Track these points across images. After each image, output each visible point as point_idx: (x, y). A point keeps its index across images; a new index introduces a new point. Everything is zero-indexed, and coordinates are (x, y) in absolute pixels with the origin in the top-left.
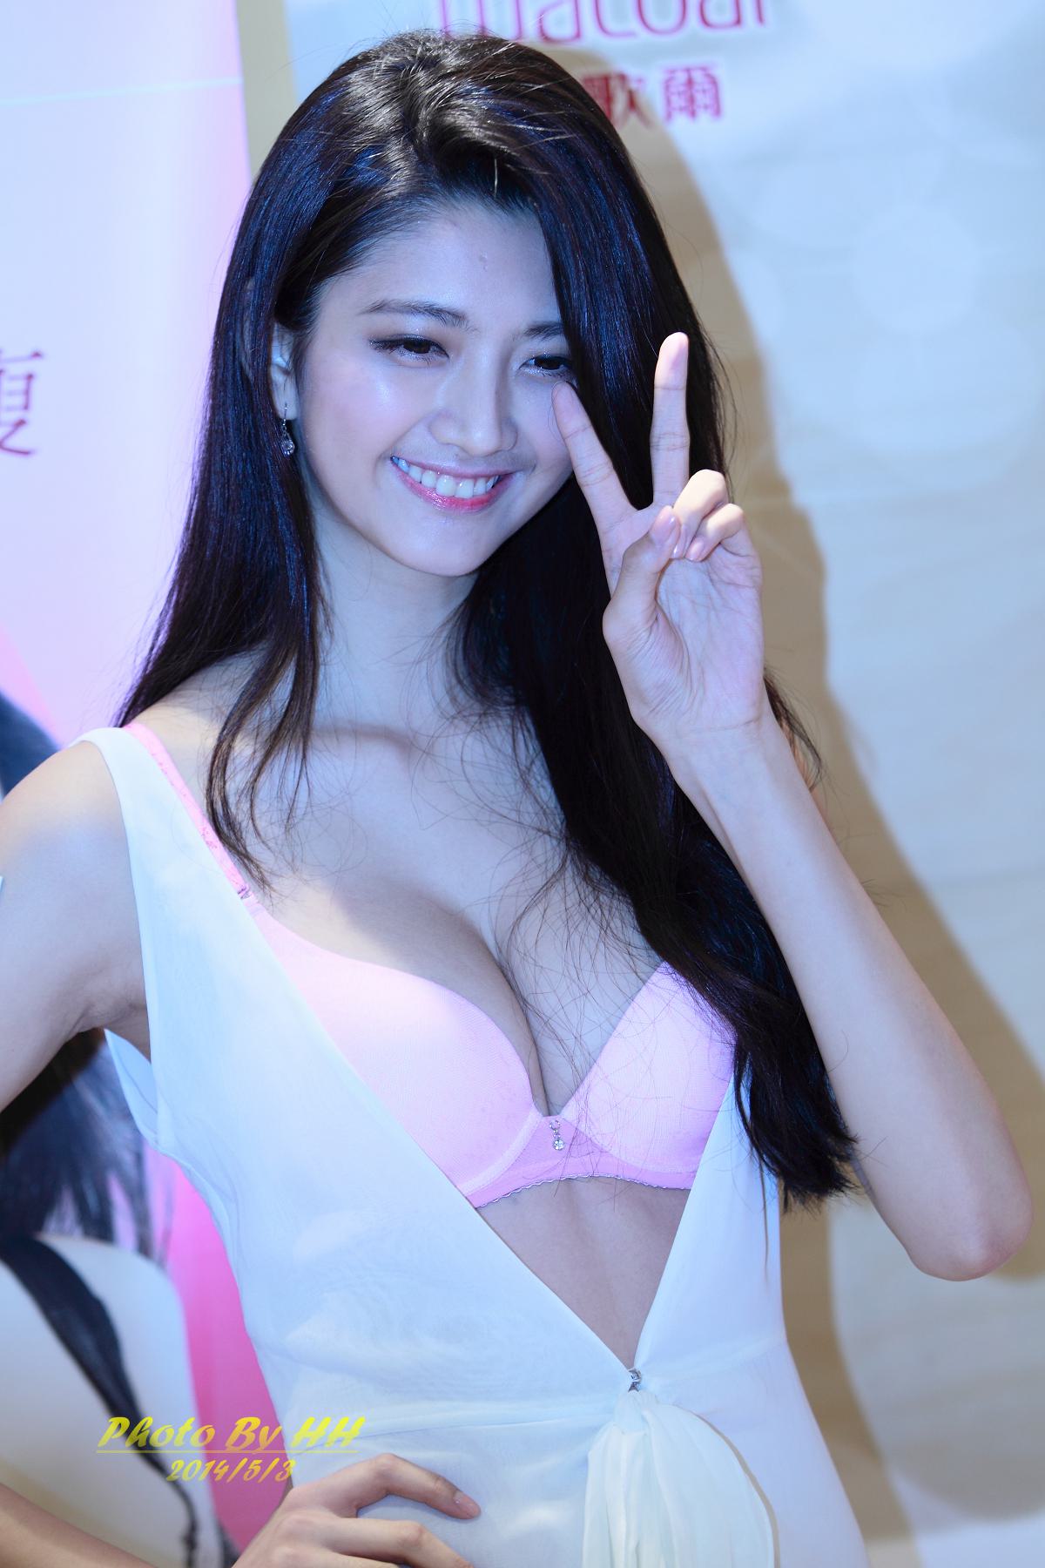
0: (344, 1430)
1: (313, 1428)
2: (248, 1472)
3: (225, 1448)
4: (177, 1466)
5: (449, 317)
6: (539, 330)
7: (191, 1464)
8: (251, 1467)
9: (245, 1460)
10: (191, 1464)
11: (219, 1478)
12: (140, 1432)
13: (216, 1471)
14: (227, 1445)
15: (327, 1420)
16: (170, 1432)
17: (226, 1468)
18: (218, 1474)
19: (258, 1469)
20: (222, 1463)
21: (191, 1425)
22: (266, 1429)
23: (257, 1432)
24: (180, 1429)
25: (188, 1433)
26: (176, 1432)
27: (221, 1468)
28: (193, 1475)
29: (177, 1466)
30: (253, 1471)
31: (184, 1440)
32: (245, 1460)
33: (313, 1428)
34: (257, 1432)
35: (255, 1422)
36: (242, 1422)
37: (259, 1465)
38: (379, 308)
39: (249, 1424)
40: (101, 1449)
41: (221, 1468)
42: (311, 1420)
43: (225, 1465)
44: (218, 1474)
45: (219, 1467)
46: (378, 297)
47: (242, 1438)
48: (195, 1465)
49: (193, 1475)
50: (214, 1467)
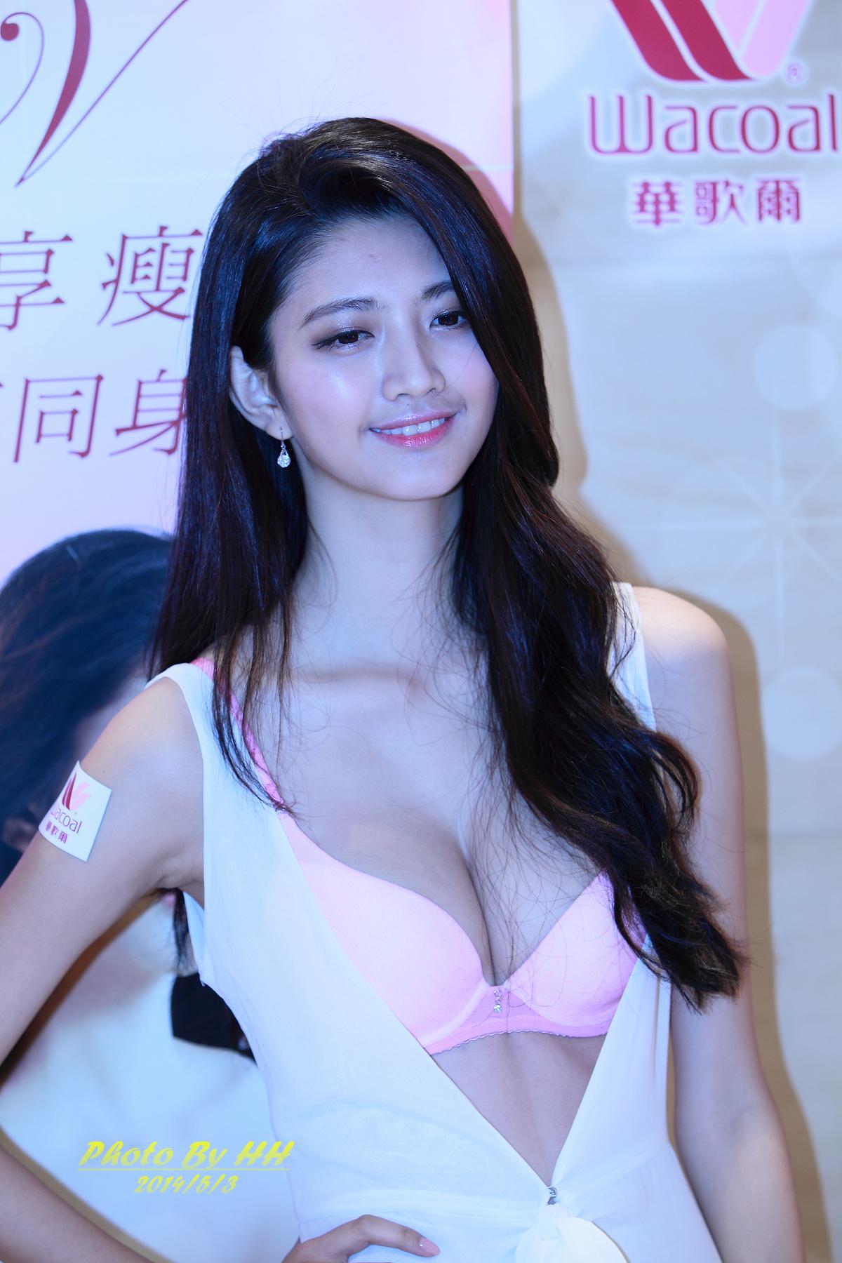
1: (253, 1150)
2: (199, 1187)
8: (203, 1181)
9: (197, 1176)
10: (154, 1179)
11: (176, 1191)
12: (113, 1153)
13: (174, 1185)
15: (263, 1144)
16: (137, 1153)
19: (208, 1184)
22: (214, 1151)
23: (207, 1153)
24: (145, 1151)
27: (178, 1182)
30: (204, 1184)
32: (197, 1176)
33: (253, 1150)
35: (206, 1145)
36: (195, 1146)
37: (210, 1180)
39: (200, 1148)
41: (178, 1182)
42: (250, 1144)
47: (195, 1159)
48: (157, 1180)
50: (173, 1181)
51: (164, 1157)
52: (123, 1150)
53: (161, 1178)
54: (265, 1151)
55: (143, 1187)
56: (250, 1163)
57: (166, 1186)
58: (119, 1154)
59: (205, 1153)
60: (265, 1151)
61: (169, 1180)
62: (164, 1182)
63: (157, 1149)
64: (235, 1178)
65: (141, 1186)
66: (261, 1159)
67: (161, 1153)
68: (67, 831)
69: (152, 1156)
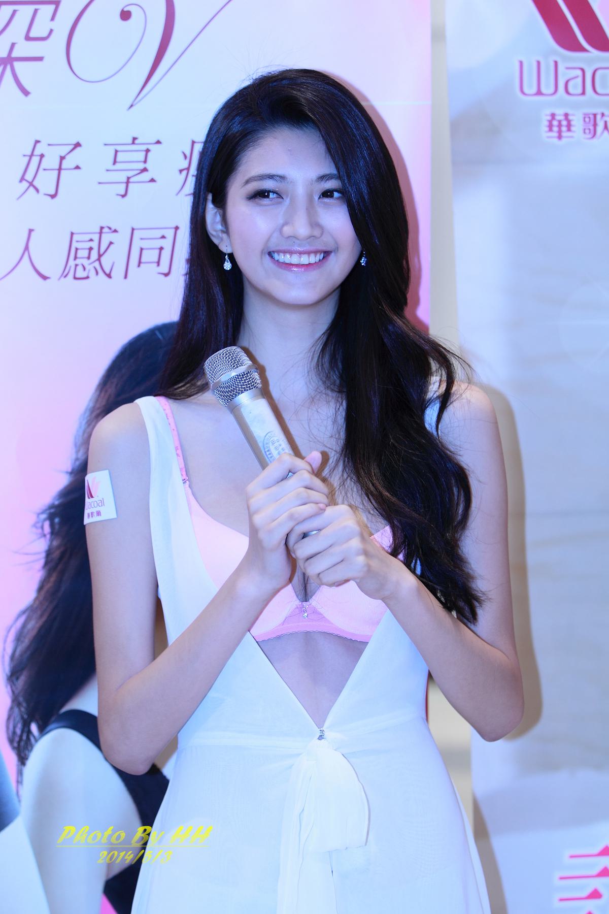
3: (131, 844)
4: (103, 854)
5: (278, 178)
6: (322, 178)
7: (111, 853)
10: (111, 853)
12: (82, 835)
13: (126, 858)
14: (132, 842)
17: (132, 855)
18: (127, 859)
21: (112, 831)
25: (109, 835)
26: (103, 835)
27: (129, 856)
29: (103, 854)
31: (107, 839)
38: (247, 182)
43: (131, 854)
45: (128, 855)
46: (246, 178)
48: (114, 854)
51: (119, 837)
52: (89, 833)
53: (116, 853)
55: (103, 859)
57: (120, 858)
58: (86, 835)
61: (122, 854)
62: (118, 855)
63: (114, 831)
64: (170, 853)
67: (117, 834)
68: (98, 509)
69: (110, 836)
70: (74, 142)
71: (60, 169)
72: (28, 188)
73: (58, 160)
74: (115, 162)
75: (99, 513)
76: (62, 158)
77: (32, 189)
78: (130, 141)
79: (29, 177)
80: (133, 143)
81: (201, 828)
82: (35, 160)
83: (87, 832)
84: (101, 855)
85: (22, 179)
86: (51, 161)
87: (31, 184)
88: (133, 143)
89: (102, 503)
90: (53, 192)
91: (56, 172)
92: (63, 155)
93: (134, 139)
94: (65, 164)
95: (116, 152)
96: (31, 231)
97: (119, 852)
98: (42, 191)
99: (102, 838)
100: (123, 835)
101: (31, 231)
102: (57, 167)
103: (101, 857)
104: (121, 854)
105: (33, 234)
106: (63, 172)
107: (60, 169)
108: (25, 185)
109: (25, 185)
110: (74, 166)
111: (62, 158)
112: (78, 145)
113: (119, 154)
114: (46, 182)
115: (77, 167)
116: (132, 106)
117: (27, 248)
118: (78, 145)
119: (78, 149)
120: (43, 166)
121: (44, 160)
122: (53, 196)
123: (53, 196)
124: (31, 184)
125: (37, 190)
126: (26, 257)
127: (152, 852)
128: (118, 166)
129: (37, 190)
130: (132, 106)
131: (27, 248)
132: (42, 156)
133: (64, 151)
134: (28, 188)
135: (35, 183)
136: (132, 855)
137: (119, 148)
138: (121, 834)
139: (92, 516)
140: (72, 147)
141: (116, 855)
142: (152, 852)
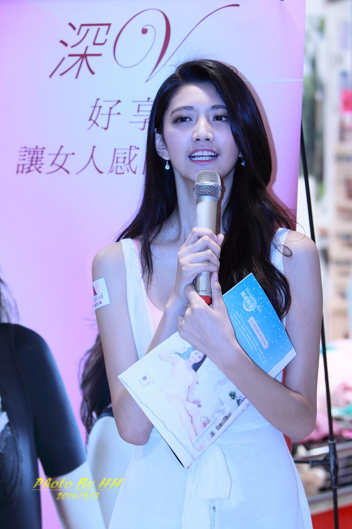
0: (116, 482)
1: (106, 482)
8: (85, 495)
11: (74, 499)
13: (73, 496)
15: (110, 479)
17: (76, 495)
18: (73, 497)
20: (75, 494)
21: (65, 481)
23: (86, 483)
24: (61, 482)
26: (59, 483)
27: (75, 495)
28: (65, 498)
30: (85, 496)
32: (83, 493)
34: (86, 483)
36: (81, 480)
37: (88, 494)
39: (84, 481)
40: (34, 489)
42: (105, 479)
43: (76, 494)
44: (73, 497)
45: (74, 495)
47: (81, 485)
48: (66, 494)
49: (65, 498)
50: (72, 495)
54: (111, 482)
55: (59, 497)
56: (104, 487)
58: (50, 483)
59: (85, 483)
60: (111, 482)
62: (68, 495)
65: (59, 497)
66: (109, 486)
67: (67, 483)
68: (100, 300)
70: (117, 100)
71: (110, 114)
72: (93, 124)
73: (109, 109)
74: (138, 111)
75: (100, 303)
76: (111, 108)
77: (95, 125)
78: (146, 100)
79: (94, 118)
80: (148, 101)
81: (116, 479)
82: (97, 109)
83: (50, 482)
84: (58, 495)
85: (90, 119)
86: (105, 110)
87: (95, 122)
88: (148, 101)
89: (102, 296)
90: (105, 127)
91: (107, 116)
92: (111, 106)
93: (149, 98)
94: (113, 111)
95: (139, 105)
96: (94, 147)
97: (69, 493)
98: (100, 125)
99: (59, 485)
100: (71, 483)
101: (94, 147)
102: (108, 113)
103: (58, 496)
104: (70, 494)
105: (95, 149)
106: (111, 116)
107: (110, 114)
108: (92, 122)
109: (92, 122)
110: (117, 113)
111: (111, 108)
112: (119, 101)
113: (141, 107)
114: (102, 121)
115: (119, 114)
116: (147, 81)
117: (92, 156)
118: (119, 101)
119: (119, 104)
120: (101, 112)
121: (102, 109)
122: (106, 129)
123: (106, 129)
124: (95, 122)
125: (98, 125)
126: (91, 161)
127: (88, 493)
128: (140, 113)
129: (98, 125)
130: (147, 81)
131: (92, 156)
132: (100, 107)
133: (112, 104)
134: (93, 124)
135: (97, 122)
136: (76, 495)
137: (140, 103)
138: (70, 483)
139: (97, 305)
140: (116, 102)
141: (67, 495)
142: (88, 493)
